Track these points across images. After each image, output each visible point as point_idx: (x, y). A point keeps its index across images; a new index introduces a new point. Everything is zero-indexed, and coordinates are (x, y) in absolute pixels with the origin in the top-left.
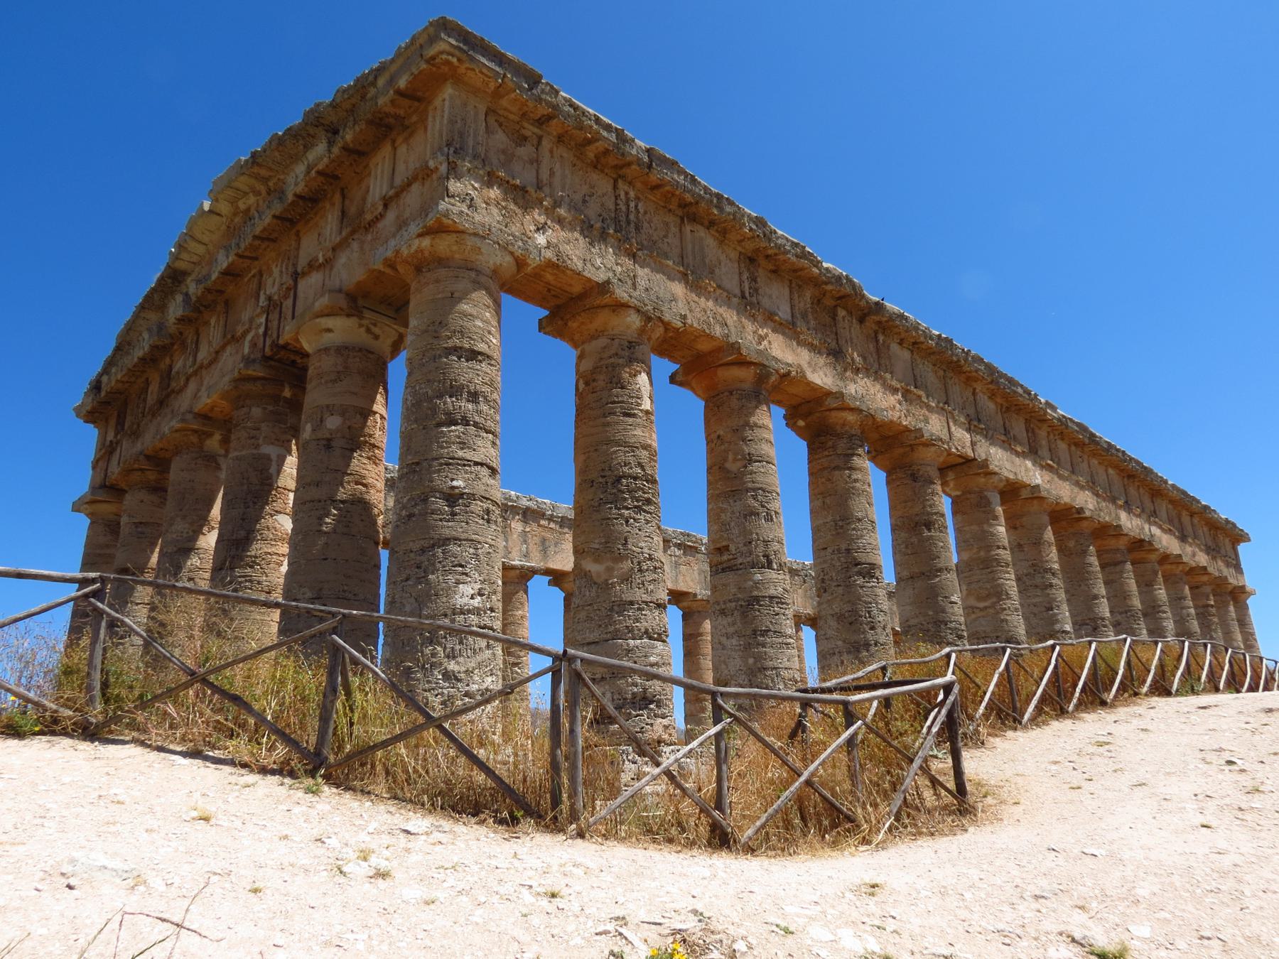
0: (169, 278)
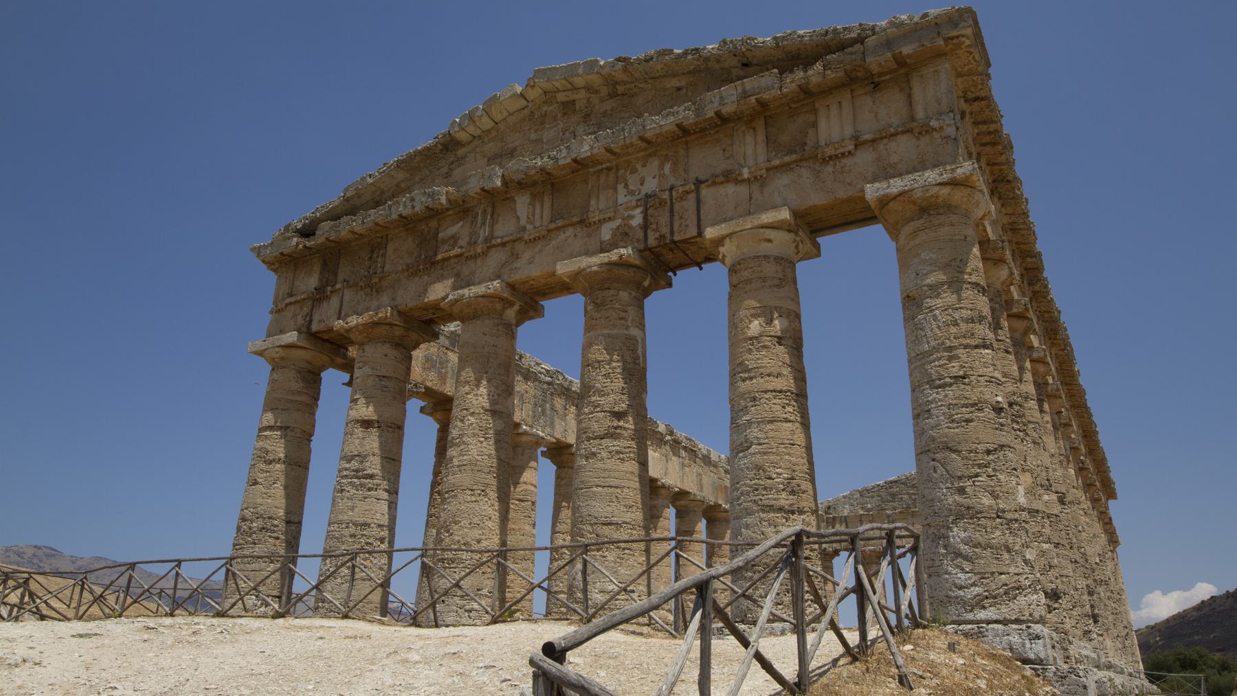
0: (441, 144)
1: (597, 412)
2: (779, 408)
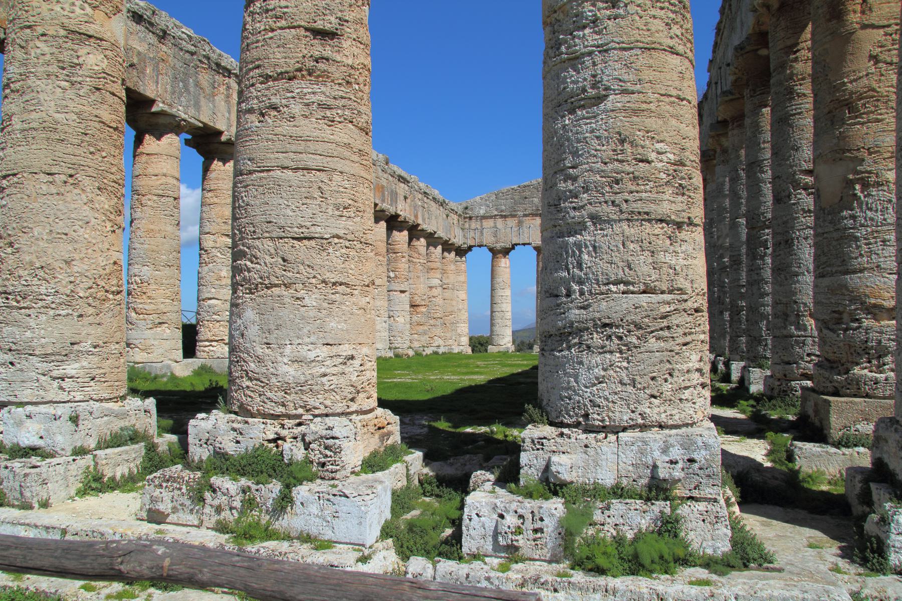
1: (282, 28)
2: (657, 25)
